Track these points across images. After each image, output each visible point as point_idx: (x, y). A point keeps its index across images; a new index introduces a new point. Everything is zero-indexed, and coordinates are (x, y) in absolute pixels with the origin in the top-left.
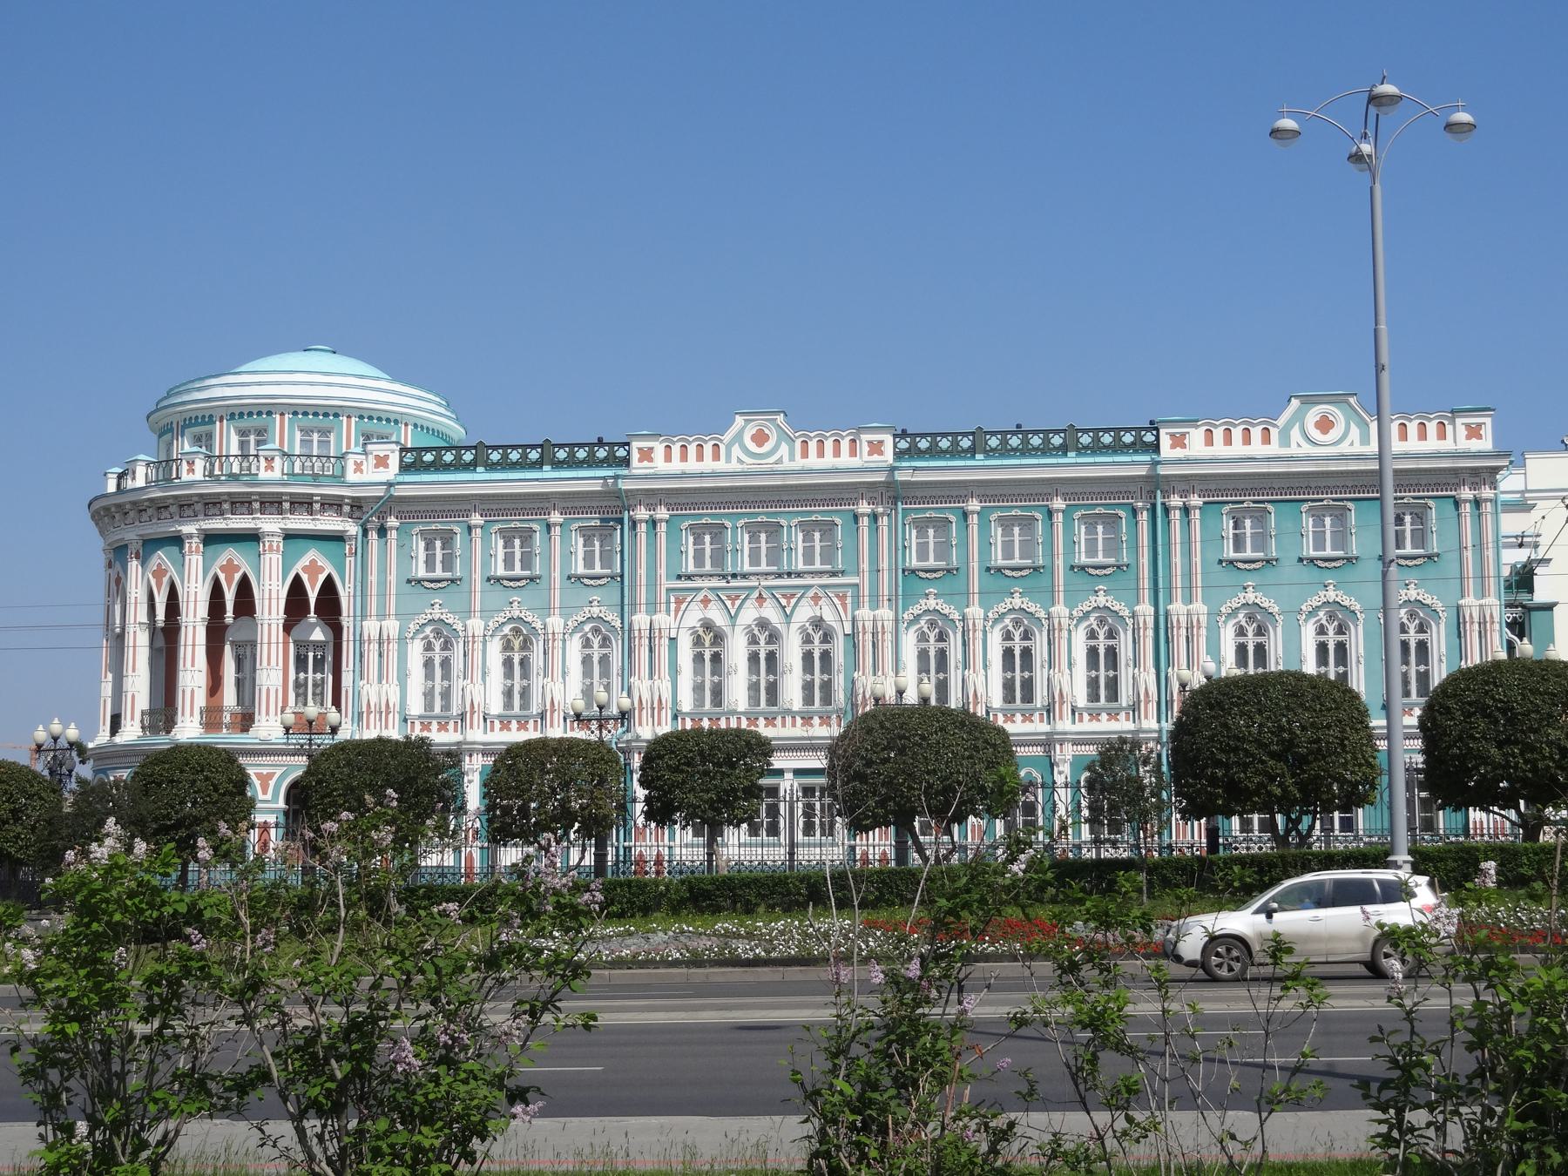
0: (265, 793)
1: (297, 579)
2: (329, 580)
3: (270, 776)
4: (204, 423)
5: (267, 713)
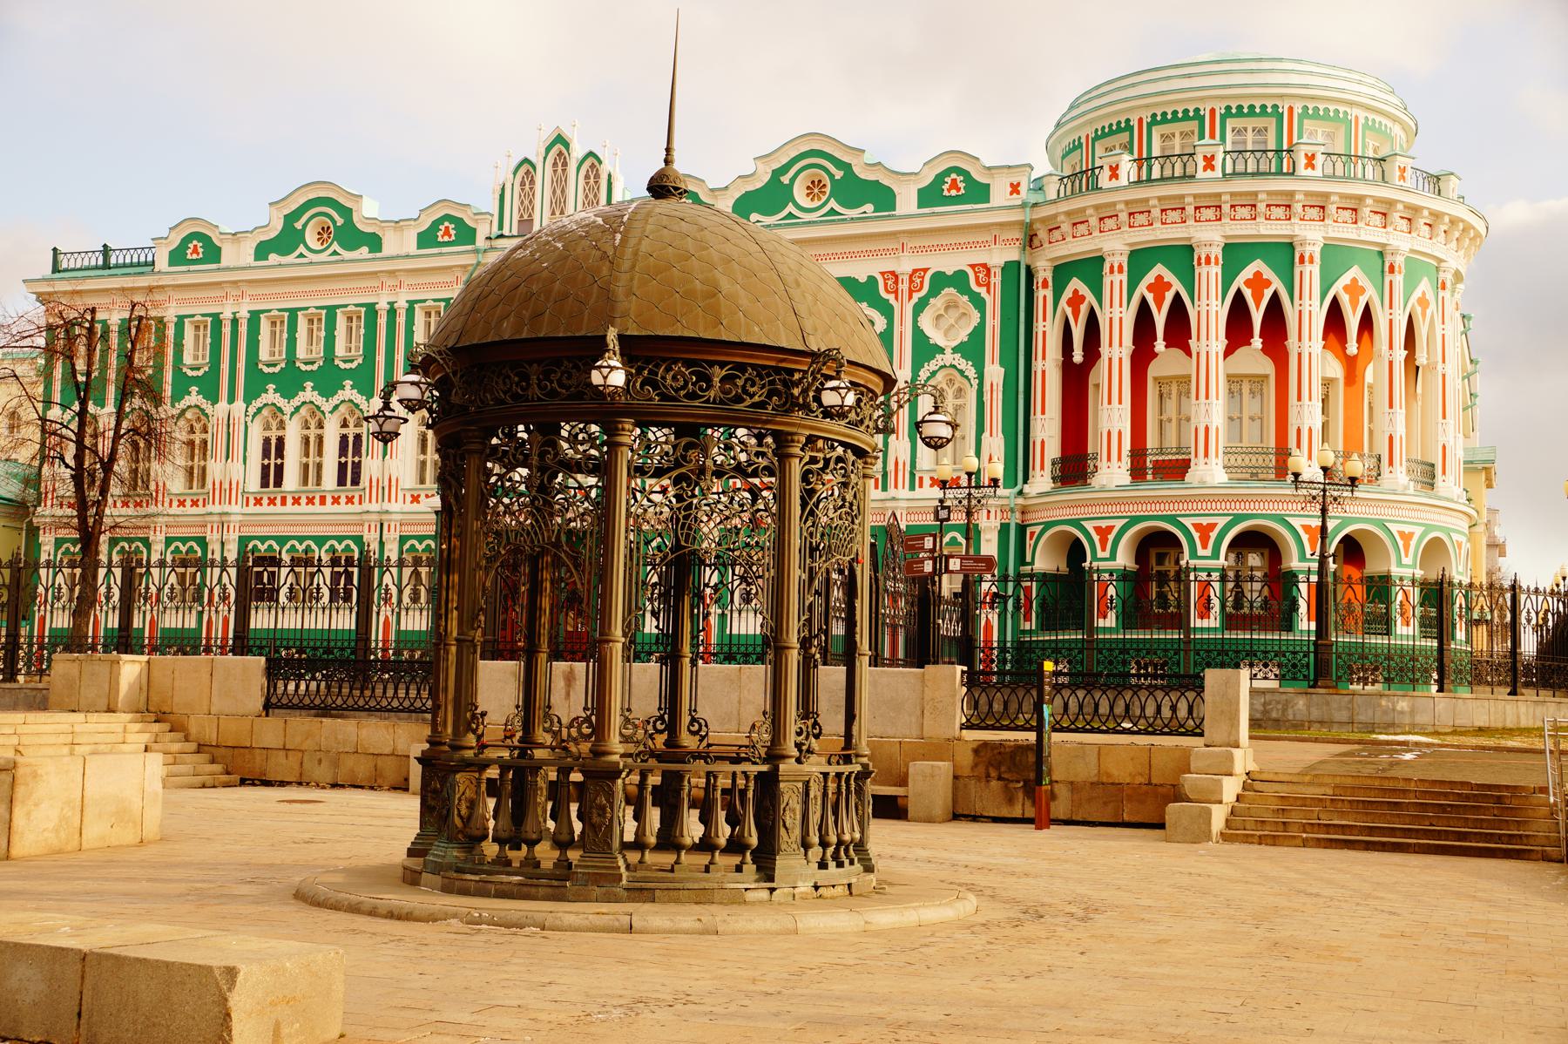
0: (1205, 547)
1: (1239, 292)
2: (1275, 297)
3: (1212, 526)
4: (1123, 130)
5: (1206, 455)
